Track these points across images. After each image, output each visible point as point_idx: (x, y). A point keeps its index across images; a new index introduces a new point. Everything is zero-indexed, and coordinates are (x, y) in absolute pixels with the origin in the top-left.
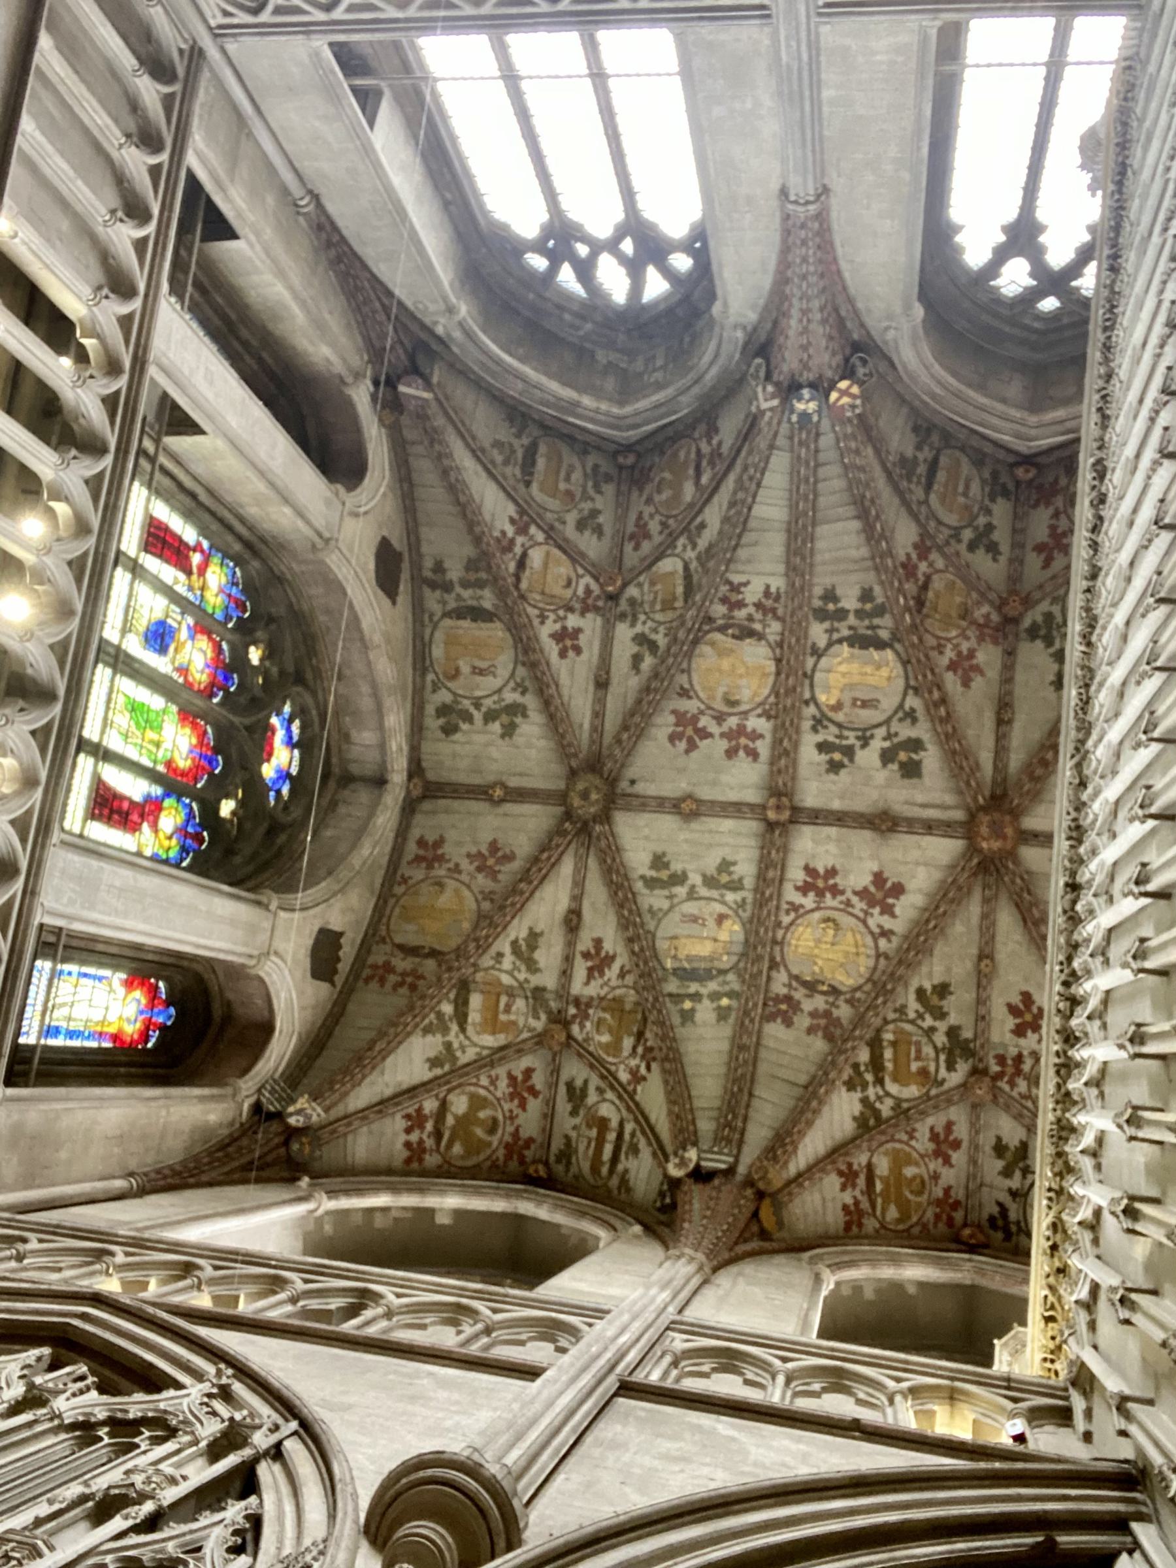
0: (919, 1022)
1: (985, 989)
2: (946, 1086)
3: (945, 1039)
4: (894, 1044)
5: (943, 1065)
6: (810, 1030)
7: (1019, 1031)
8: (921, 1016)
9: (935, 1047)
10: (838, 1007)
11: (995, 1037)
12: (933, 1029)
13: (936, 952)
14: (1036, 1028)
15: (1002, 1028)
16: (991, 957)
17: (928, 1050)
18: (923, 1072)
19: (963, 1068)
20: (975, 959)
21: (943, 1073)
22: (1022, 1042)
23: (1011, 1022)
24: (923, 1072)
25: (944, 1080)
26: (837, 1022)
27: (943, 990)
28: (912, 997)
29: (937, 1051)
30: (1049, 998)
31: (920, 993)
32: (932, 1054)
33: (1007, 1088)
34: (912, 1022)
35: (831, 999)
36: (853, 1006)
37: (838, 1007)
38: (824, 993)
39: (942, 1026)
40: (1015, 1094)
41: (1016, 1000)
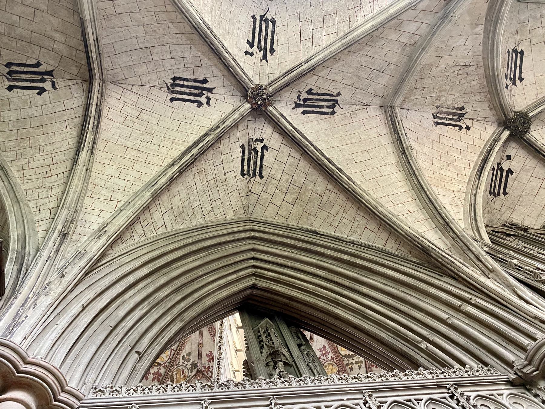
0: (183, 365)
3: (190, 366)
4: (176, 374)
5: (190, 372)
6: (153, 380)
7: (209, 361)
8: (183, 363)
10: (161, 369)
11: (203, 361)
12: (186, 365)
14: (213, 361)
15: (205, 360)
18: (185, 376)
19: (195, 371)
20: (198, 344)
21: (190, 374)
22: (210, 363)
23: (207, 358)
26: (160, 375)
27: (189, 354)
28: (181, 358)
29: (188, 370)
30: (216, 354)
31: (183, 358)
33: (206, 374)
34: (182, 366)
35: (159, 367)
36: (165, 368)
38: (157, 366)
39: (189, 363)
40: (208, 376)
41: (208, 353)
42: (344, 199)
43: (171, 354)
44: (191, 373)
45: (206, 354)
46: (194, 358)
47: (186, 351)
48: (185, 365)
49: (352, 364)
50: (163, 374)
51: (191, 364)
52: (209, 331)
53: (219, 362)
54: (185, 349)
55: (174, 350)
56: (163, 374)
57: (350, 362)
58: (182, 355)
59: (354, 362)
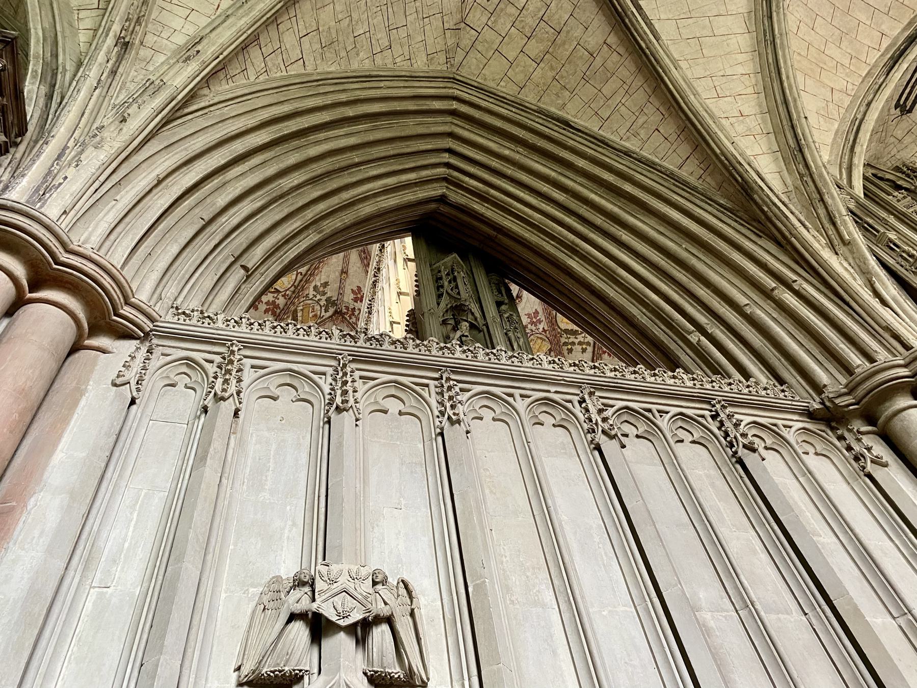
0: (314, 298)
1: (343, 284)
2: (324, 318)
3: (325, 302)
4: (302, 310)
5: (323, 311)
6: (266, 311)
7: (356, 300)
9: (320, 306)
10: (278, 299)
11: (345, 299)
13: (323, 270)
14: (361, 301)
15: (348, 297)
16: (346, 273)
17: (317, 307)
18: (315, 316)
19: (331, 311)
20: (340, 271)
21: (323, 314)
22: (355, 304)
23: (352, 296)
24: (315, 316)
25: (323, 316)
26: (277, 306)
27: (325, 284)
28: (311, 289)
30: (366, 291)
31: (315, 288)
32: (319, 309)
33: (348, 318)
34: (311, 299)
35: (276, 295)
36: (286, 298)
37: (278, 299)
39: (324, 298)
40: (351, 321)
41: (355, 289)
42: (633, 68)
43: (296, 279)
44: (325, 312)
45: (352, 290)
46: (331, 292)
47: (320, 279)
48: (316, 299)
49: (573, 343)
50: (281, 307)
51: (326, 300)
52: (360, 255)
53: (370, 304)
54: (319, 275)
55: (301, 274)
56: (281, 307)
57: (571, 340)
58: (313, 284)
59: (576, 341)
